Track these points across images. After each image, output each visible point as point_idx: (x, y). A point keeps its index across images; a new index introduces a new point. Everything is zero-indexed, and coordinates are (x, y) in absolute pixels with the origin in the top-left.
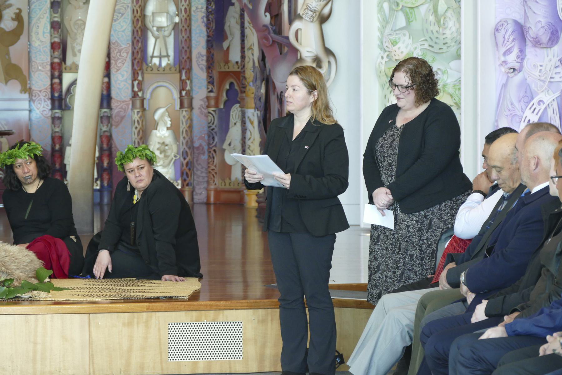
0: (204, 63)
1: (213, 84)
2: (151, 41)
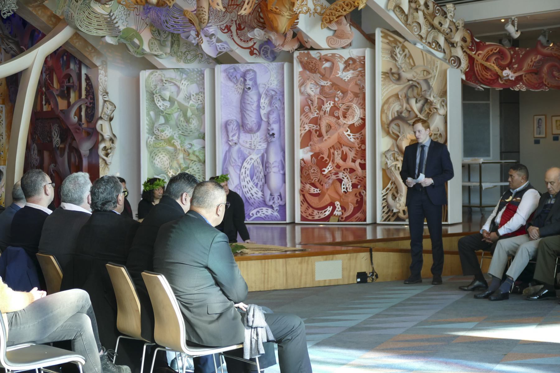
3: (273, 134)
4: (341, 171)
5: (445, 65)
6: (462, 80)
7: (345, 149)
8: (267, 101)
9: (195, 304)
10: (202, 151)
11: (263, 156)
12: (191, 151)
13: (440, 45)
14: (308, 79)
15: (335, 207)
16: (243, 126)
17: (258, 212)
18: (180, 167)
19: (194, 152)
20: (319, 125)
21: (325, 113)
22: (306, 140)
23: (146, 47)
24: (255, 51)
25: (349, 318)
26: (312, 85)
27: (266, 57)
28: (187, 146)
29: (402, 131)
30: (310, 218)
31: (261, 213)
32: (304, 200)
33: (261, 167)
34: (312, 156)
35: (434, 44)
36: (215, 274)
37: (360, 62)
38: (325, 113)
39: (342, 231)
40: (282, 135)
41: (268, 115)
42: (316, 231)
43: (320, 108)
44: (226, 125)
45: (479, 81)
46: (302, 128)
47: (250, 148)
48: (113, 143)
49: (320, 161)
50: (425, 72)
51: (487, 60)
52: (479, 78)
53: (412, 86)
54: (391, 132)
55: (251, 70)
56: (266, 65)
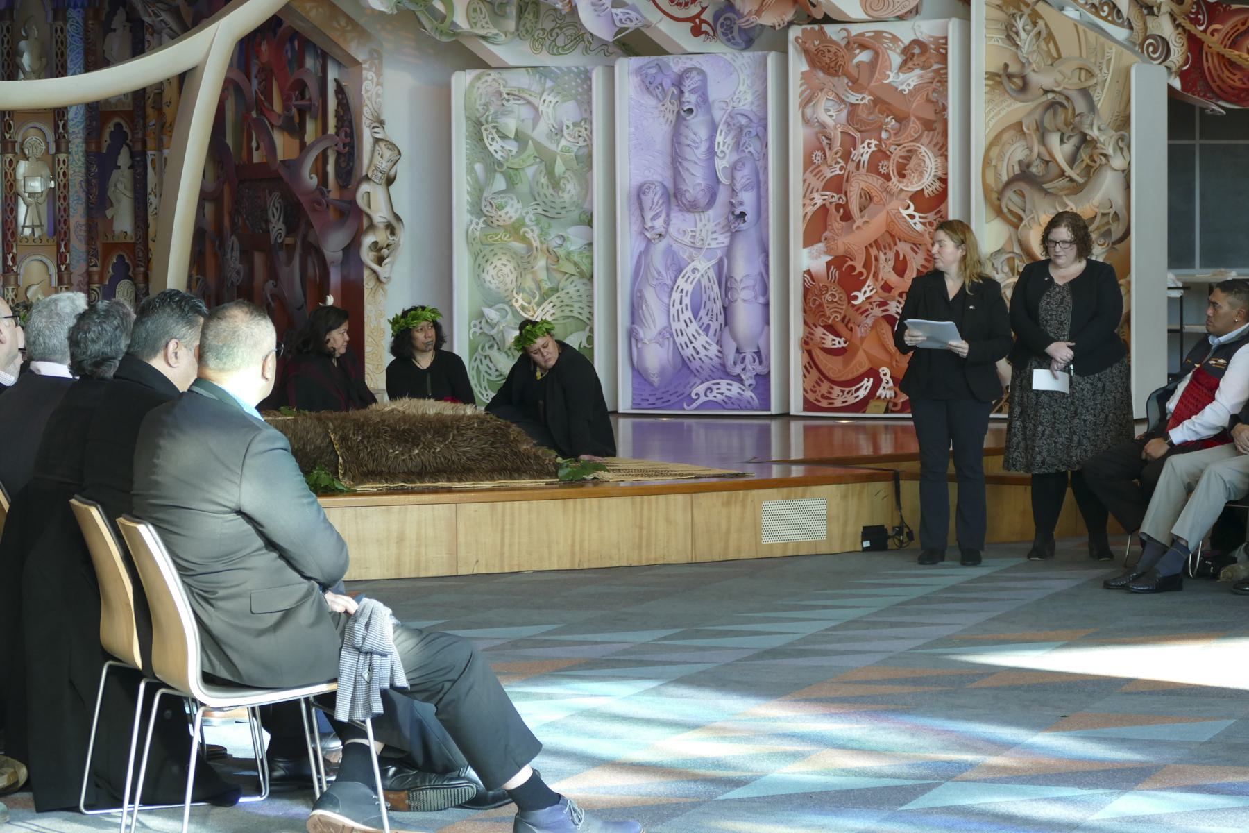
0: (83, 233)
1: (96, 256)
2: (22, 209)
3: (743, 214)
4: (893, 299)
5: (1128, 57)
6: (1170, 88)
7: (904, 248)
8: (730, 140)
9: (221, 593)
10: (587, 254)
11: (719, 266)
12: (561, 253)
13: (1119, 11)
14: (821, 90)
15: (881, 380)
16: (675, 196)
17: (710, 389)
18: (539, 288)
19: (569, 253)
20: (846, 194)
21: (858, 167)
22: (816, 229)
23: (460, 20)
24: (705, 27)
25: (777, 630)
26: (831, 103)
27: (729, 40)
28: (554, 242)
29: (1028, 206)
30: (824, 404)
31: (715, 392)
32: (811, 364)
33: (716, 287)
34: (829, 264)
35: (1106, 8)
36: (262, 526)
37: (937, 50)
38: (858, 167)
39: (895, 433)
40: (763, 216)
41: (734, 168)
42: (838, 435)
43: (847, 156)
44: (640, 193)
45: (1212, 91)
46: (808, 201)
47: (693, 246)
48: (393, 233)
49: (846, 275)
50: (1083, 73)
51: (1234, 45)
52: (1213, 86)
53: (1052, 106)
54: (1005, 210)
55: (695, 68)
56: (728, 57)
